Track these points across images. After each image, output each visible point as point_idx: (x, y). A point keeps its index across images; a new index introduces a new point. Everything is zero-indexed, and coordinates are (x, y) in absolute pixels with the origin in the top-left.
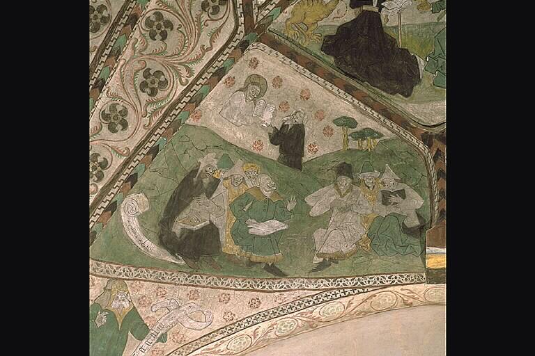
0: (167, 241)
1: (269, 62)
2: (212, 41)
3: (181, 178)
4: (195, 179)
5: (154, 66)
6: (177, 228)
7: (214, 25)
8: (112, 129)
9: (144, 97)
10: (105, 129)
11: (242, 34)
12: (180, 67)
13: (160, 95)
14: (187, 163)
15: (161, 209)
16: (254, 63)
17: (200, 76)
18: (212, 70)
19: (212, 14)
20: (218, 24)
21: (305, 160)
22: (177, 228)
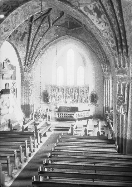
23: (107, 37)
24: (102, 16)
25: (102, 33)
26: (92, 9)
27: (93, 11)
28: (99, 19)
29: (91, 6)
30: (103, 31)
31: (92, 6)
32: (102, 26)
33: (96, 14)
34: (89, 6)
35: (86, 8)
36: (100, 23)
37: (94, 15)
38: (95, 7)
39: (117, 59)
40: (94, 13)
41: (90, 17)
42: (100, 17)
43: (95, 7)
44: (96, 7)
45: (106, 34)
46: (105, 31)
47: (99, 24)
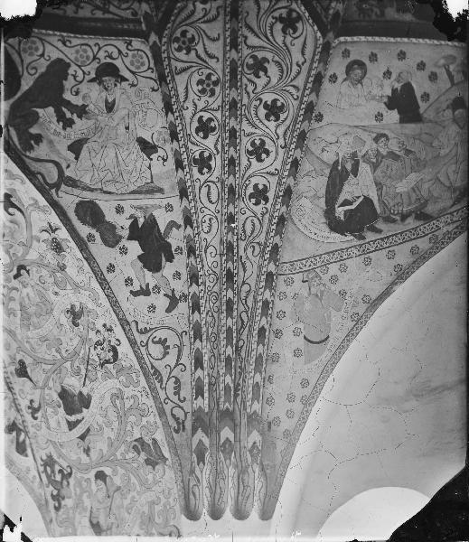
0: (335, 226)
1: (360, 46)
2: (303, 54)
3: (327, 172)
4: (340, 168)
5: (268, 98)
6: (340, 212)
7: (299, 42)
8: (260, 160)
9: (272, 124)
10: (254, 161)
11: (321, 39)
12: (288, 88)
13: (282, 117)
14: (329, 157)
15: (322, 203)
16: (346, 53)
17: (305, 89)
18: (311, 79)
19: (294, 32)
20: (302, 39)
21: (421, 111)
22: (340, 212)
23: (156, 364)
24: (168, 269)
25: (139, 338)
26: (122, 223)
27: (126, 233)
28: (148, 274)
29: (119, 210)
30: (145, 331)
31: (129, 211)
32: (152, 308)
33: (135, 248)
34: (107, 207)
35: (90, 212)
36: (145, 292)
37: (124, 251)
38: (141, 221)
39: (205, 473)
40: (124, 242)
41: (98, 249)
42: (155, 267)
43: (141, 221)
44: (151, 222)
45: (156, 350)
46: (161, 334)
47: (135, 294)
